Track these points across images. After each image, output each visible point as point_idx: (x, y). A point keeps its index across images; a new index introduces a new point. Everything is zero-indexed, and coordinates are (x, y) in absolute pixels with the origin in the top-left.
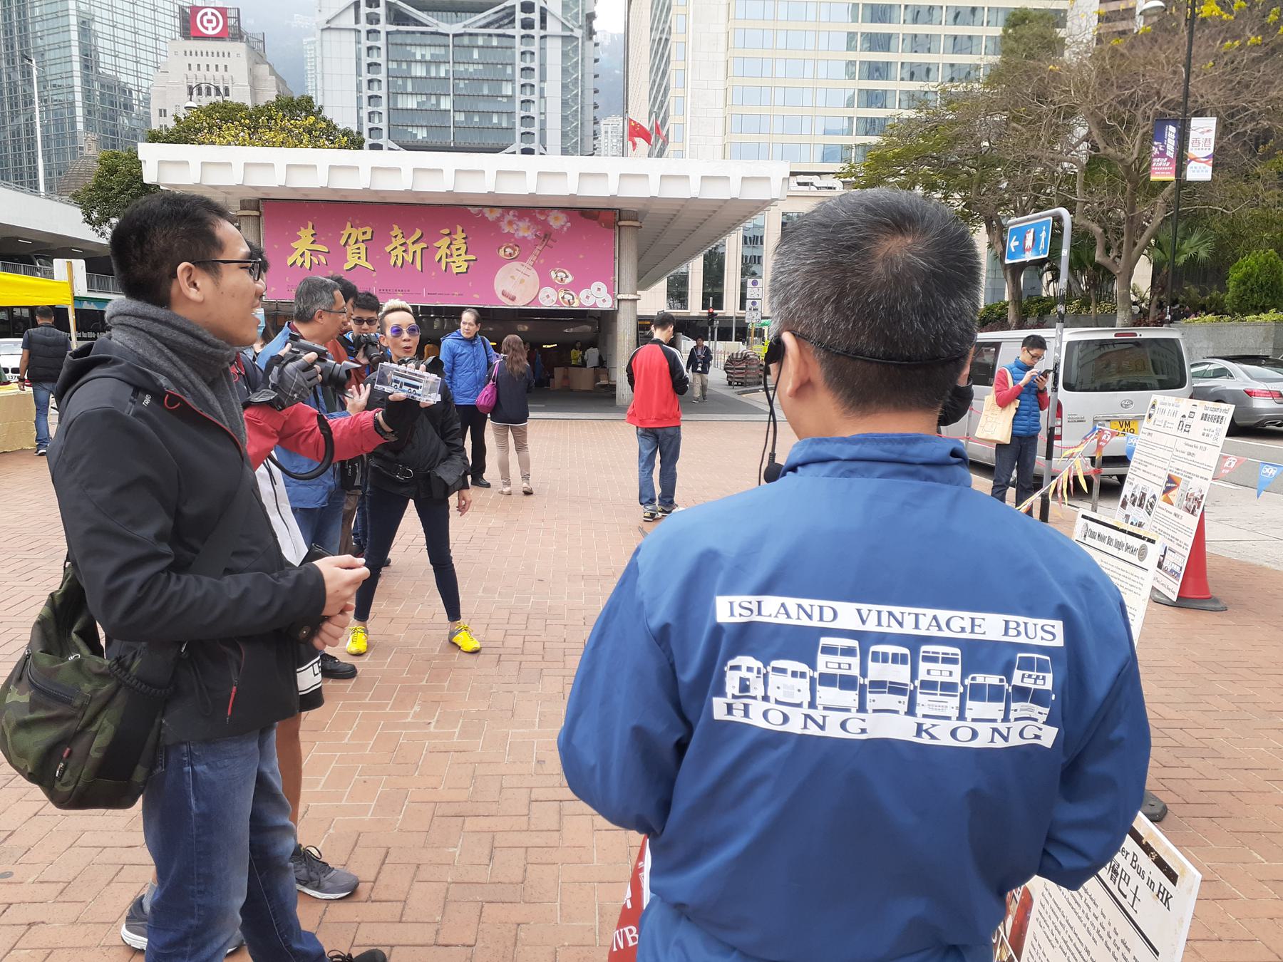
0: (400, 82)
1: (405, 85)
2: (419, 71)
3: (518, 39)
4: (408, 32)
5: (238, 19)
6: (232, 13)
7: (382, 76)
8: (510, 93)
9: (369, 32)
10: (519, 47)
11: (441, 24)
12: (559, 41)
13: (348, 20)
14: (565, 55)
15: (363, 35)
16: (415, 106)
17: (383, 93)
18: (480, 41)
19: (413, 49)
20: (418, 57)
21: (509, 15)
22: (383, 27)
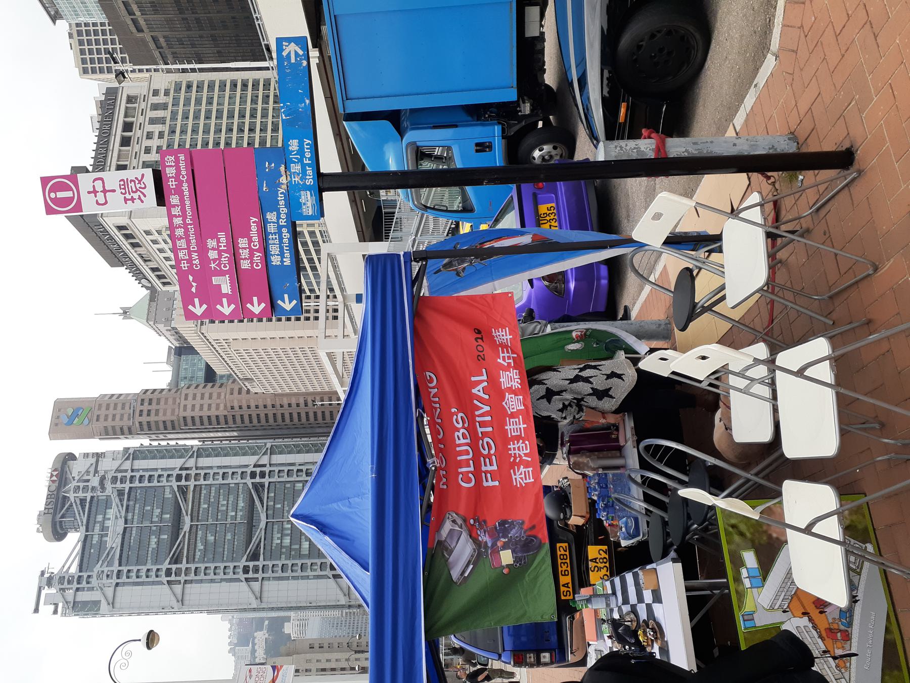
0: (293, 553)
2: (287, 541)
3: (271, 480)
7: (290, 563)
8: (301, 485)
10: (275, 479)
11: (261, 526)
12: (273, 456)
13: (256, 585)
14: (280, 453)
17: (299, 562)
18: (272, 503)
19: (274, 545)
20: (279, 541)
21: (258, 487)
22: (260, 563)
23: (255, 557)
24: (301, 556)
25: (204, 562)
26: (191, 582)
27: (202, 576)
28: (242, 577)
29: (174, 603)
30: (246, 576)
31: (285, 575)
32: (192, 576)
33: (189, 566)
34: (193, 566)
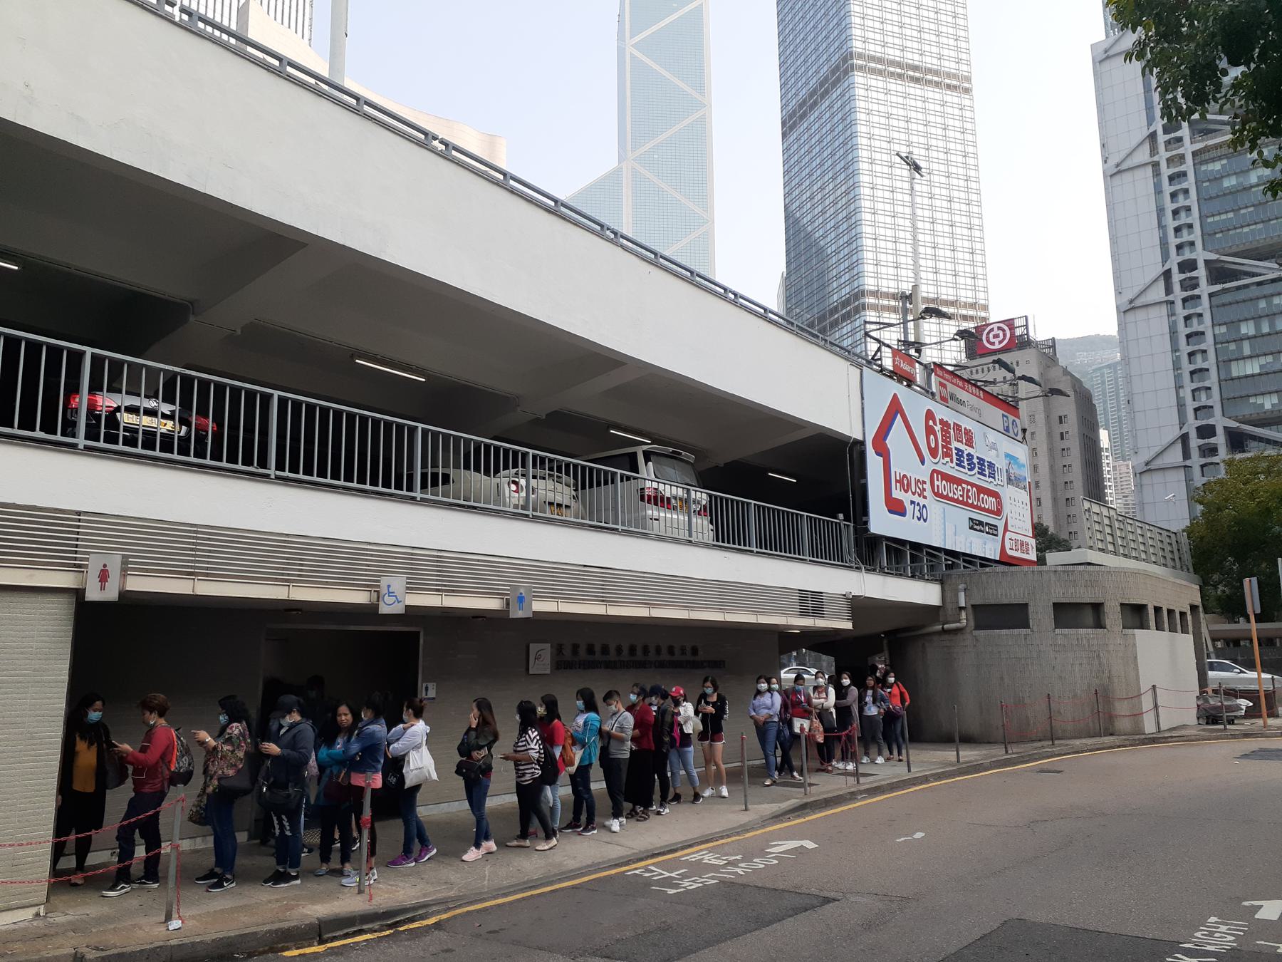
0: (1232, 346)
1: (1240, 349)
4: (1238, 288)
5: (1026, 326)
6: (1017, 323)
7: (1208, 343)
9: (1185, 300)
13: (1158, 293)
15: (1179, 304)
16: (1257, 371)
17: (1211, 363)
22: (1204, 289)
23: (1218, 273)
24: (1224, 363)
25: (1198, 183)
26: (1157, 174)
27: (1168, 189)
28: (1173, 264)
29: (1113, 161)
30: (1175, 270)
31: (1183, 341)
32: (1166, 172)
33: (1189, 158)
34: (1188, 166)
